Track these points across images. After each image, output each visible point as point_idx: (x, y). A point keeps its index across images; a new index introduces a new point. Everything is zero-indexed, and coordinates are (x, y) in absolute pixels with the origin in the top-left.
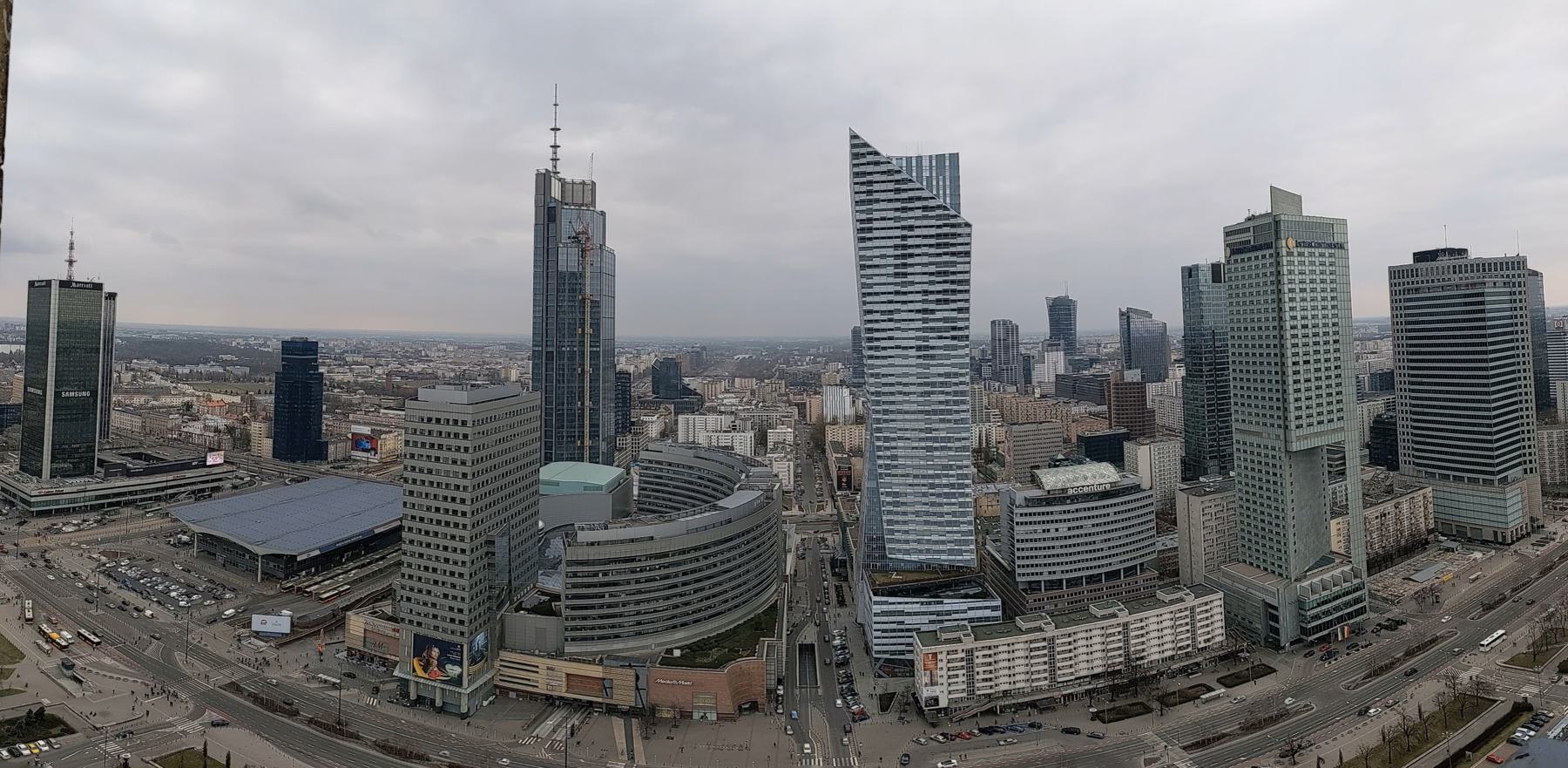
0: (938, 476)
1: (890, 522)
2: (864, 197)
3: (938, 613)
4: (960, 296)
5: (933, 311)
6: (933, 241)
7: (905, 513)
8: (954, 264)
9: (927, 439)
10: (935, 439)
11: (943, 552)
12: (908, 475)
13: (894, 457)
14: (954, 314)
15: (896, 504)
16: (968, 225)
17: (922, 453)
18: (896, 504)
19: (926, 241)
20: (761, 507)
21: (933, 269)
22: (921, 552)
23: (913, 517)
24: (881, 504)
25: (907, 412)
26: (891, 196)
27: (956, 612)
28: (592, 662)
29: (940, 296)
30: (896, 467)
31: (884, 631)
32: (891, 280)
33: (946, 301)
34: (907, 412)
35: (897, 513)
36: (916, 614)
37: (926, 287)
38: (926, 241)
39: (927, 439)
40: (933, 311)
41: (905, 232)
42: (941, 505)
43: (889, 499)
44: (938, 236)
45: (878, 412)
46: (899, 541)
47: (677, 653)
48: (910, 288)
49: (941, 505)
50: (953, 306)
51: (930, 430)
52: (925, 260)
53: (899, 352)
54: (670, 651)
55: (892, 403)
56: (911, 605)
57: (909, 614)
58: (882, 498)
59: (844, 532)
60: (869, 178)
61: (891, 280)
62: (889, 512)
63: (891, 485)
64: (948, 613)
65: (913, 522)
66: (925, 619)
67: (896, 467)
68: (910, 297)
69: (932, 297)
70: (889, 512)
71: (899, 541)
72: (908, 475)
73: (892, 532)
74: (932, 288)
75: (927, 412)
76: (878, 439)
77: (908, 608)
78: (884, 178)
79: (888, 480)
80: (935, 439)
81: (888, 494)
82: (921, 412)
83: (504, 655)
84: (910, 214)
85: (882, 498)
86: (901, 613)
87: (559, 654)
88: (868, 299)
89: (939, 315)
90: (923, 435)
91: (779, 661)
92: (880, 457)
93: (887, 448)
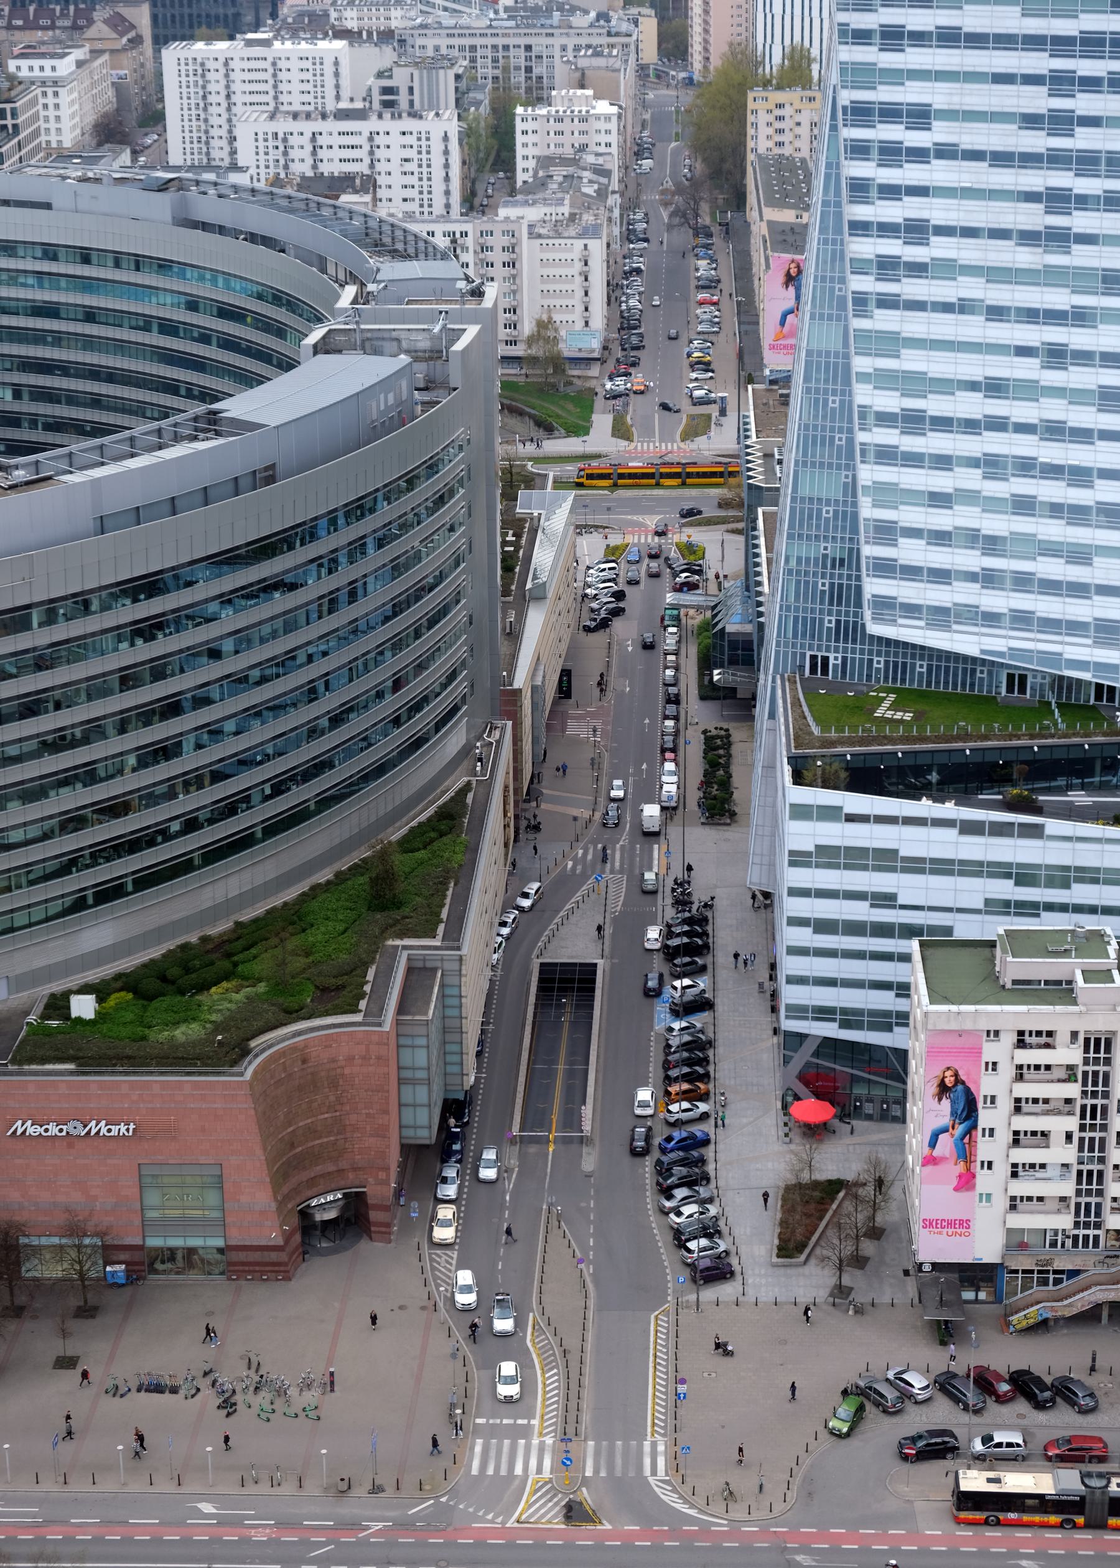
0: (1080, 317)
1: (886, 494)
3: (1024, 876)
7: (943, 462)
9: (1056, 159)
10: (1086, 163)
11: (1075, 627)
12: (963, 307)
13: (917, 231)
15: (913, 422)
17: (1033, 217)
18: (913, 422)
20: (401, 418)
22: (991, 619)
23: (970, 479)
24: (848, 415)
25: (977, 40)
27: (1090, 876)
30: (918, 269)
31: (824, 926)
34: (977, 40)
35: (913, 460)
36: (942, 867)
39: (1056, 159)
42: (1083, 435)
43: (890, 401)
45: (861, 37)
46: (911, 572)
49: (1083, 435)
51: (1061, 123)
56: (926, 827)
57: (916, 866)
58: (864, 395)
62: (886, 455)
63: (892, 343)
64: (1063, 877)
65: (970, 497)
66: (974, 891)
67: (918, 269)
70: (886, 455)
71: (911, 572)
72: (963, 307)
73: (887, 532)
75: (1060, 45)
76: (860, 150)
77: (913, 842)
79: (884, 320)
80: (1086, 163)
81: (883, 380)
82: (1034, 42)
85: (864, 395)
86: (886, 859)
90: (1037, 141)
91: (450, 1030)
92: (860, 228)
93: (891, 192)
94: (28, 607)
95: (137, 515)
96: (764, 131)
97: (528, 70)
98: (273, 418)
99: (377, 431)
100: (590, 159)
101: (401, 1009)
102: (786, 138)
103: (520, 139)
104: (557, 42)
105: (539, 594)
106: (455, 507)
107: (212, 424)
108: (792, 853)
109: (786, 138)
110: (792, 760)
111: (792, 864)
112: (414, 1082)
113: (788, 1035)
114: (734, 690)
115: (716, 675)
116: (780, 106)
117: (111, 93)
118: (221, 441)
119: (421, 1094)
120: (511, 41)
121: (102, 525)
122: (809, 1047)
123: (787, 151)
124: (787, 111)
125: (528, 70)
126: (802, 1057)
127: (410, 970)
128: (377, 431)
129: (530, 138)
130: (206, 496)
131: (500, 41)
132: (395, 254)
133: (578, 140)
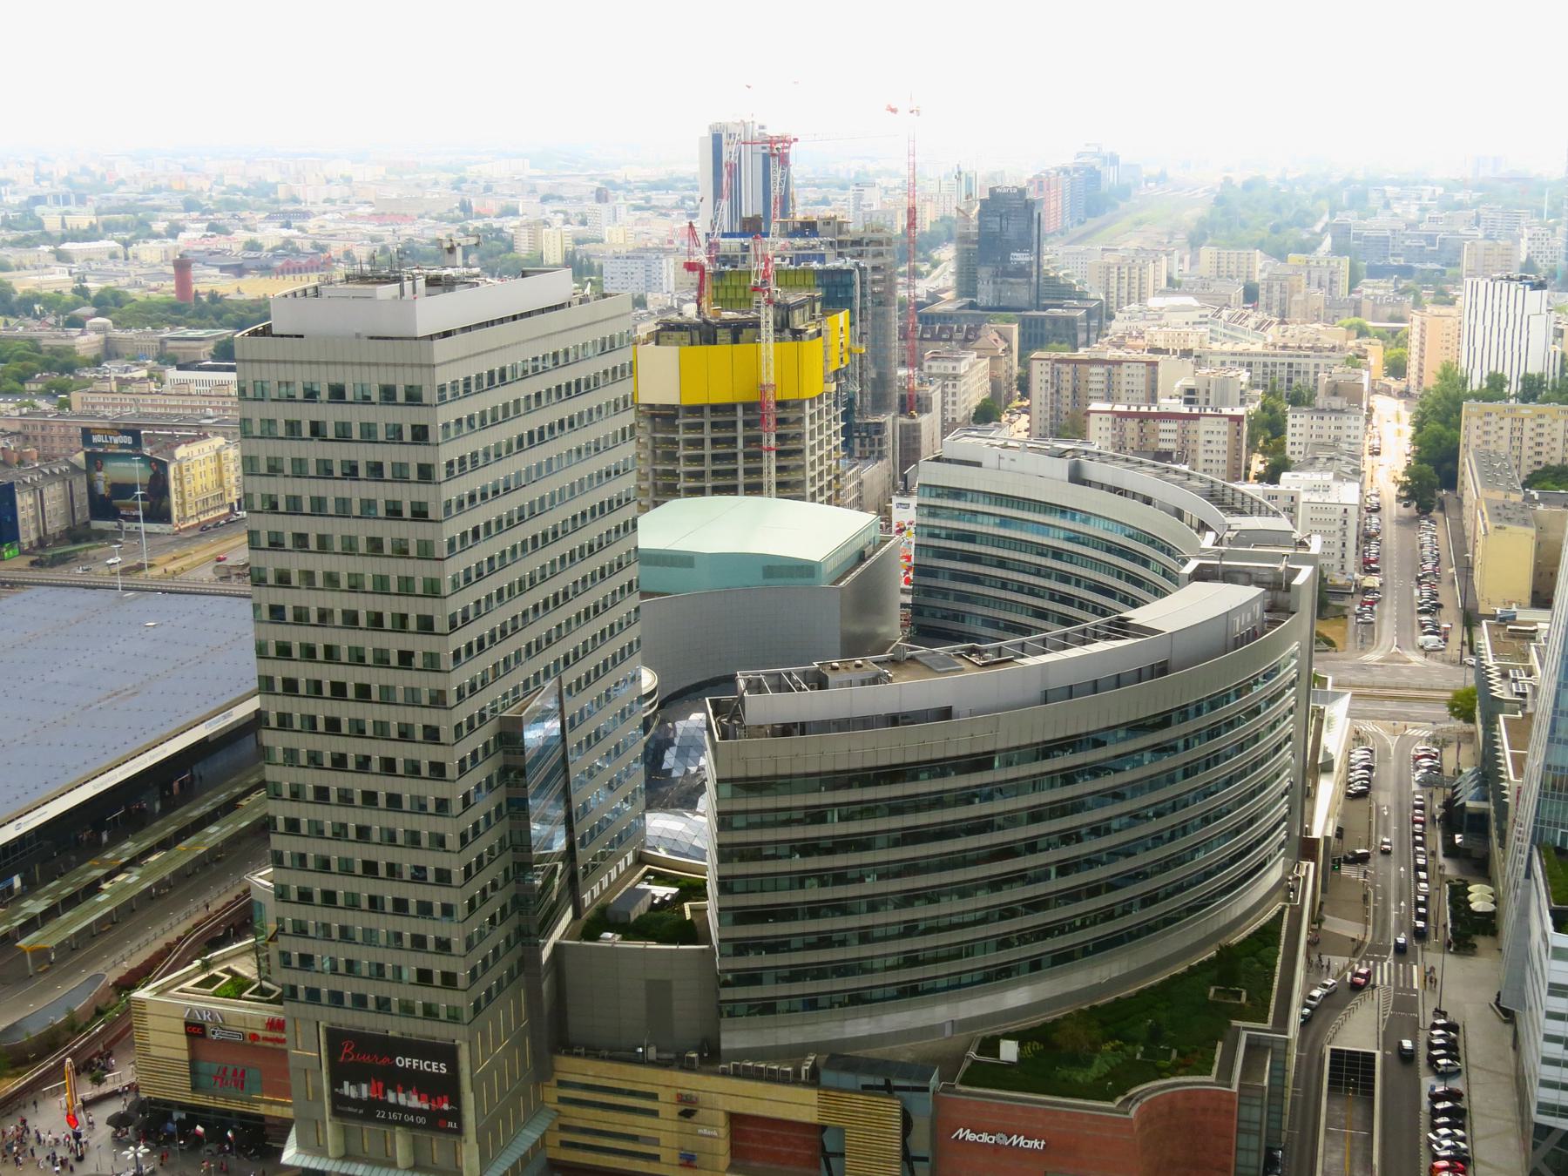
28: (793, 1079)
47: (1009, 1051)
54: (990, 1046)
59: (1490, 724)
83: (575, 1068)
87: (710, 1056)
94: (993, 752)
95: (1070, 692)
96: (1475, 432)
97: (1290, 381)
98: (1168, 628)
99: (1240, 642)
100: (1345, 446)
101: (1243, 1076)
102: (1492, 438)
103: (1290, 430)
104: (1312, 362)
105: (1327, 768)
106: (1289, 698)
107: (1122, 628)
108: (1551, 985)
109: (1492, 438)
110: (1553, 913)
111: (1551, 993)
112: (1248, 1132)
113: (1538, 1126)
114: (1469, 851)
115: (1458, 839)
116: (1541, 416)
117: (988, 385)
118: (1131, 641)
119: (1253, 1142)
120: (1278, 360)
121: (1046, 698)
122: (1552, 1141)
123: (1492, 447)
124: (1494, 418)
125: (1290, 381)
126: (1547, 1145)
127: (1248, 1046)
128: (1240, 642)
129: (1297, 430)
130: (1118, 681)
131: (1269, 360)
132: (1241, 513)
133: (1334, 432)
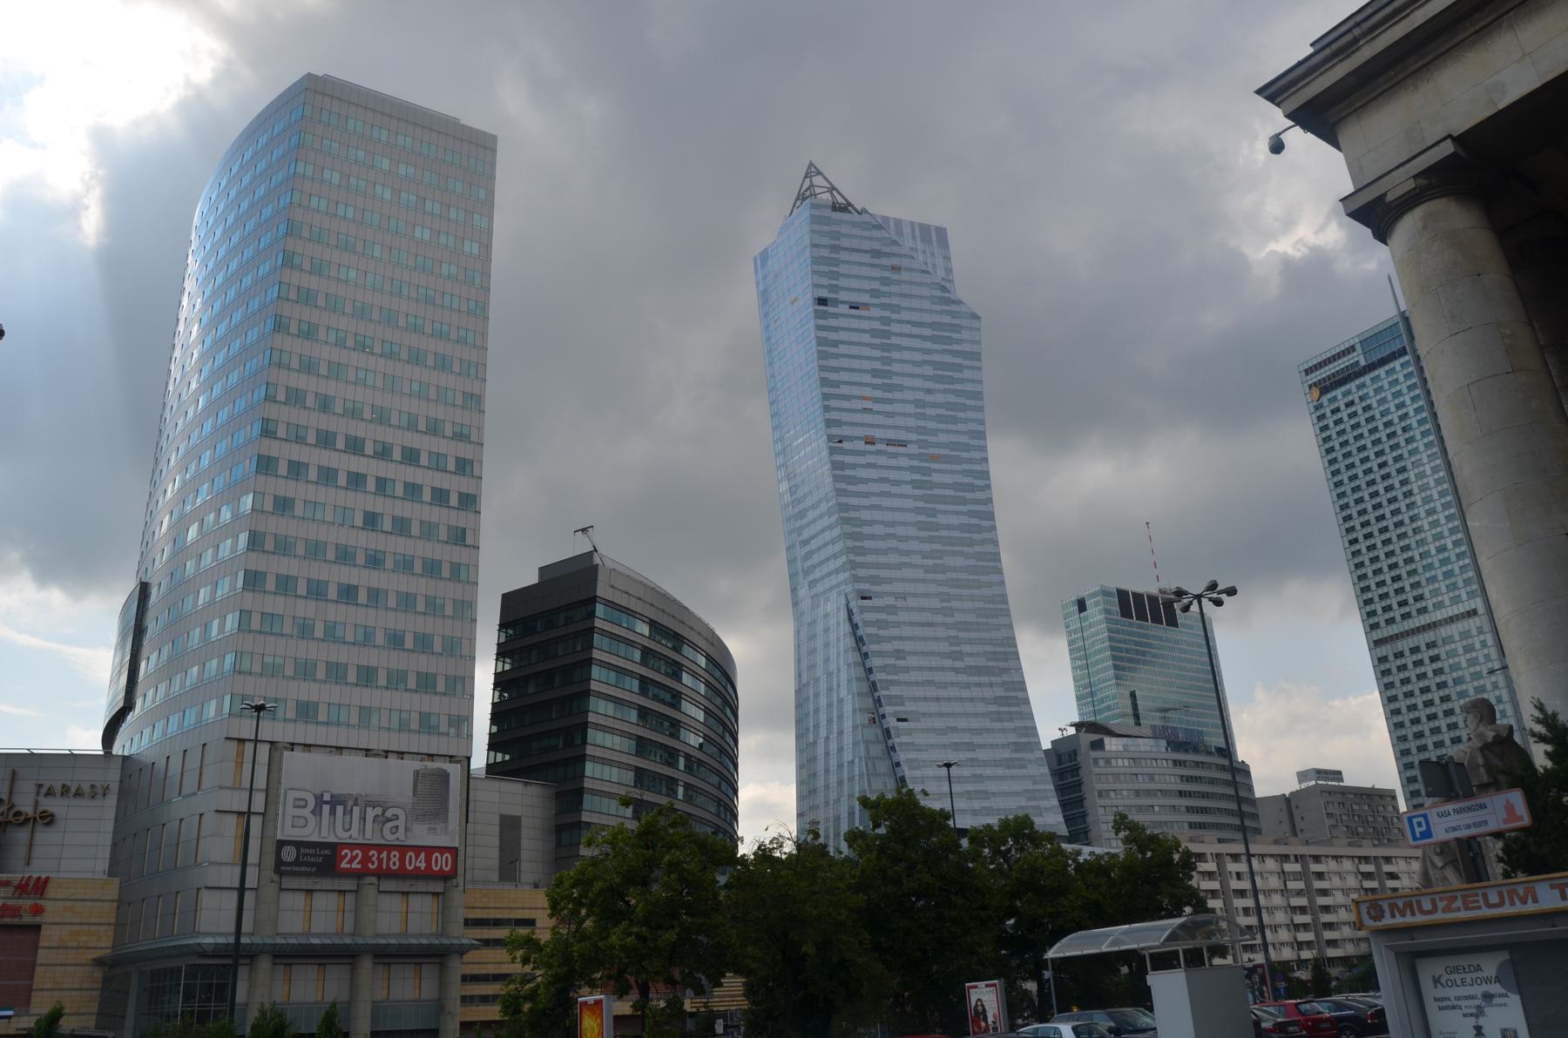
2: (825, 253)
4: (971, 415)
5: (935, 432)
6: (927, 332)
8: (960, 368)
14: (964, 439)
16: (975, 317)
19: (916, 331)
21: (928, 370)
26: (867, 259)
29: (942, 412)
32: (867, 378)
33: (955, 420)
37: (920, 396)
38: (916, 331)
40: (935, 432)
41: (887, 314)
44: (932, 325)
48: (897, 395)
50: (961, 427)
52: (918, 357)
53: (886, 487)
55: (887, 566)
60: (834, 228)
61: (867, 378)
68: (898, 408)
69: (928, 411)
74: (929, 398)
78: (858, 232)
84: (895, 289)
88: (833, 403)
89: (943, 438)
